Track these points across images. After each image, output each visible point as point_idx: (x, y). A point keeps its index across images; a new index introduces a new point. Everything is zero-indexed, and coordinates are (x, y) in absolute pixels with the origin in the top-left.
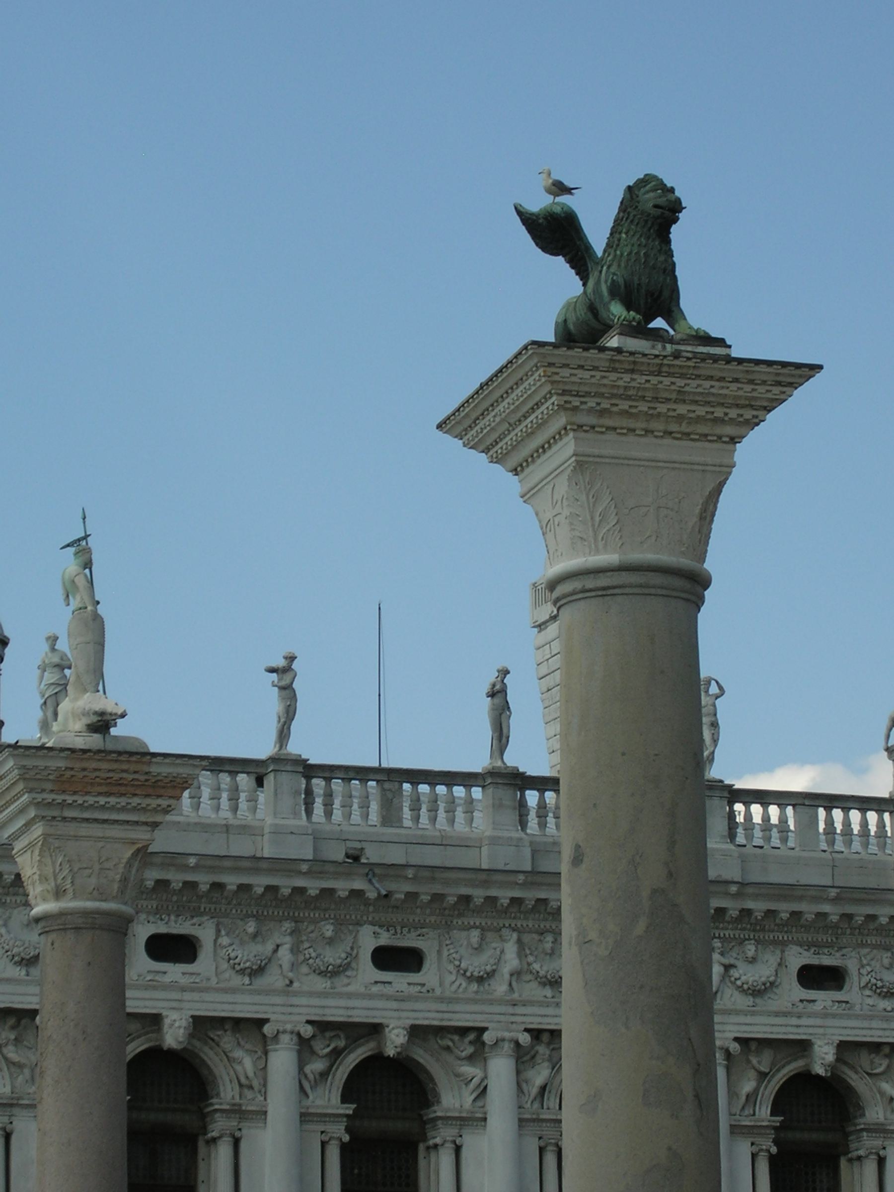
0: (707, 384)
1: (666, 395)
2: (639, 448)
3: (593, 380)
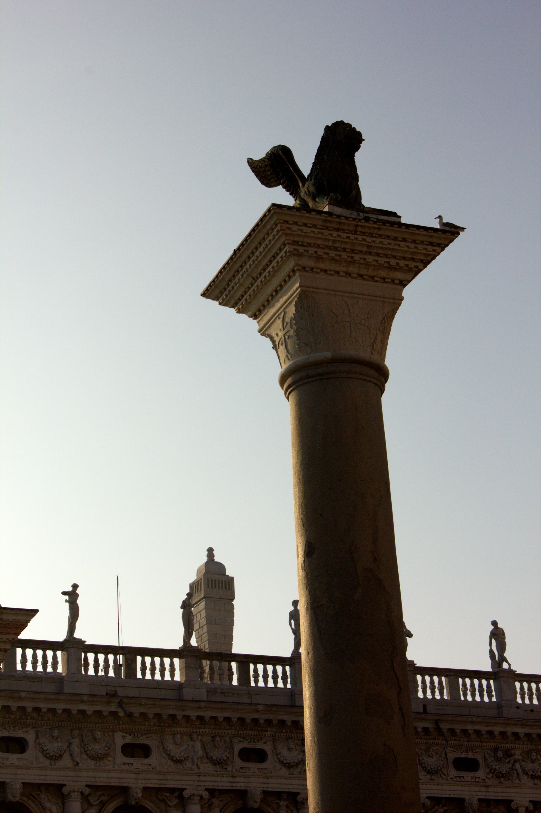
0: (386, 241)
1: (359, 248)
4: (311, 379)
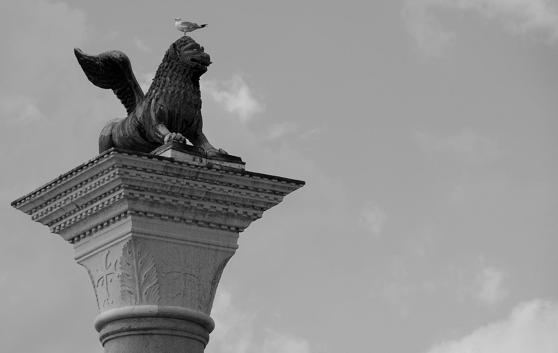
1: (198, 194)
2: (176, 230)
3: (151, 180)
4: (132, 333)
